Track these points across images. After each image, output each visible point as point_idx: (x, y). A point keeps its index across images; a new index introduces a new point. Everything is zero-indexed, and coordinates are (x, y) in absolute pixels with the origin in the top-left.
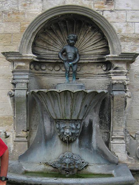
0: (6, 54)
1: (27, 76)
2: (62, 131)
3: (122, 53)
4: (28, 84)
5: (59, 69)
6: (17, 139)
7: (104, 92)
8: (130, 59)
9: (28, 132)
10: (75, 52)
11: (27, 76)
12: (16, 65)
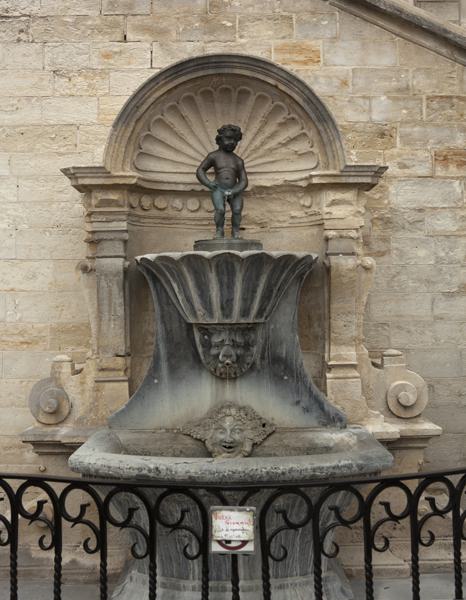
0: (72, 171)
1: (125, 224)
2: (214, 351)
3: (347, 166)
4: (125, 242)
5: (198, 205)
6: (103, 376)
7: (309, 256)
8: (368, 180)
9: (129, 359)
10: (237, 166)
11: (125, 224)
12: (96, 198)
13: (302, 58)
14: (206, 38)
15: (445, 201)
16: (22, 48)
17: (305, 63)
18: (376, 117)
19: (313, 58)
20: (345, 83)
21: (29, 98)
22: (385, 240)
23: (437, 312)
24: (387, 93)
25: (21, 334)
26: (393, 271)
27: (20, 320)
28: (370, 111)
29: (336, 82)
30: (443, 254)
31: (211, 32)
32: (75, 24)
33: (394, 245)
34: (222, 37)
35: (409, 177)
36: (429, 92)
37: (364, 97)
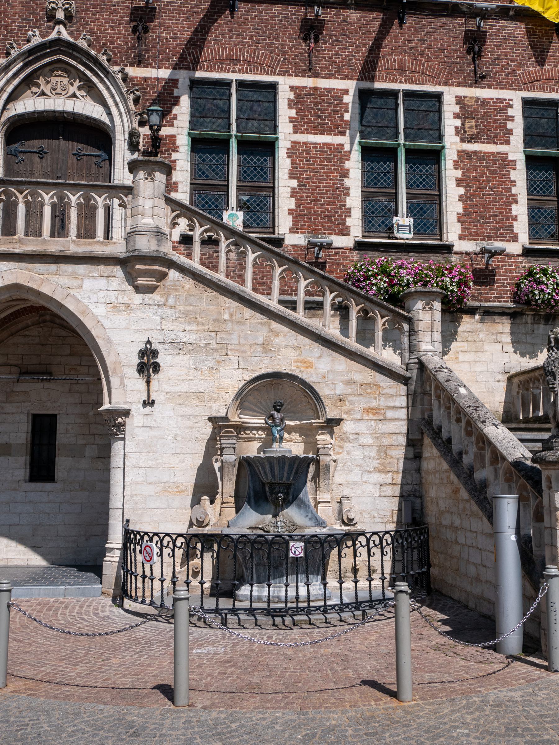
13: (305, 365)
14: (263, 355)
15: (368, 430)
16: (181, 357)
17: (307, 368)
18: (338, 392)
19: (310, 365)
20: (324, 377)
21: (183, 380)
22: (342, 447)
23: (364, 480)
24: (342, 382)
25: (177, 488)
26: (345, 461)
27: (177, 481)
28: (335, 389)
29: (320, 376)
30: (366, 454)
31: (265, 353)
32: (204, 347)
33: (345, 449)
34: (270, 355)
35: (352, 419)
36: (361, 381)
37: (333, 383)
